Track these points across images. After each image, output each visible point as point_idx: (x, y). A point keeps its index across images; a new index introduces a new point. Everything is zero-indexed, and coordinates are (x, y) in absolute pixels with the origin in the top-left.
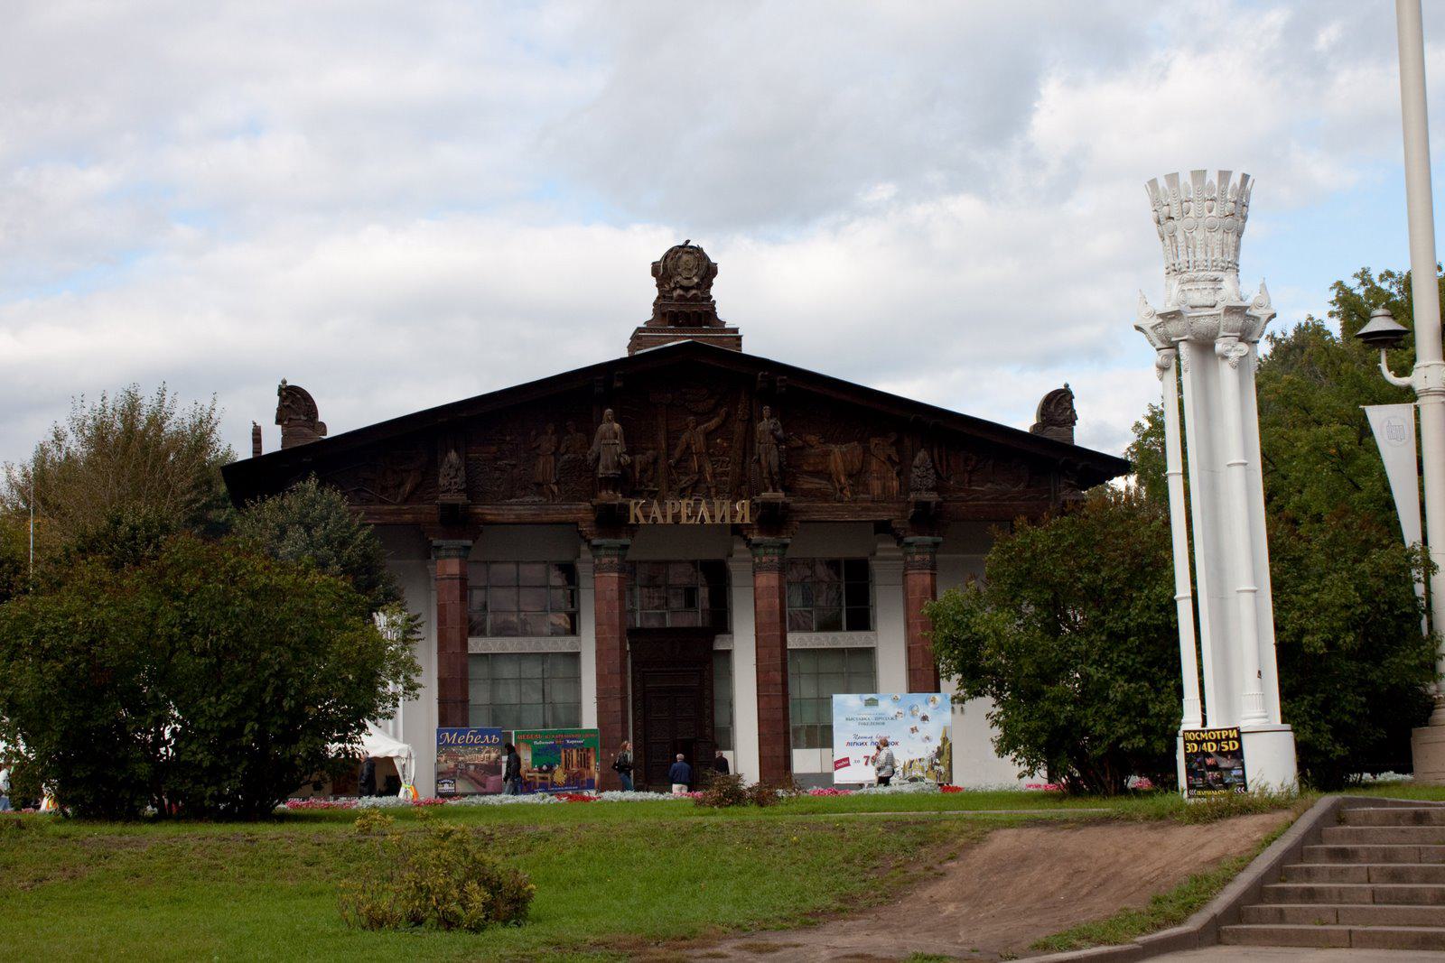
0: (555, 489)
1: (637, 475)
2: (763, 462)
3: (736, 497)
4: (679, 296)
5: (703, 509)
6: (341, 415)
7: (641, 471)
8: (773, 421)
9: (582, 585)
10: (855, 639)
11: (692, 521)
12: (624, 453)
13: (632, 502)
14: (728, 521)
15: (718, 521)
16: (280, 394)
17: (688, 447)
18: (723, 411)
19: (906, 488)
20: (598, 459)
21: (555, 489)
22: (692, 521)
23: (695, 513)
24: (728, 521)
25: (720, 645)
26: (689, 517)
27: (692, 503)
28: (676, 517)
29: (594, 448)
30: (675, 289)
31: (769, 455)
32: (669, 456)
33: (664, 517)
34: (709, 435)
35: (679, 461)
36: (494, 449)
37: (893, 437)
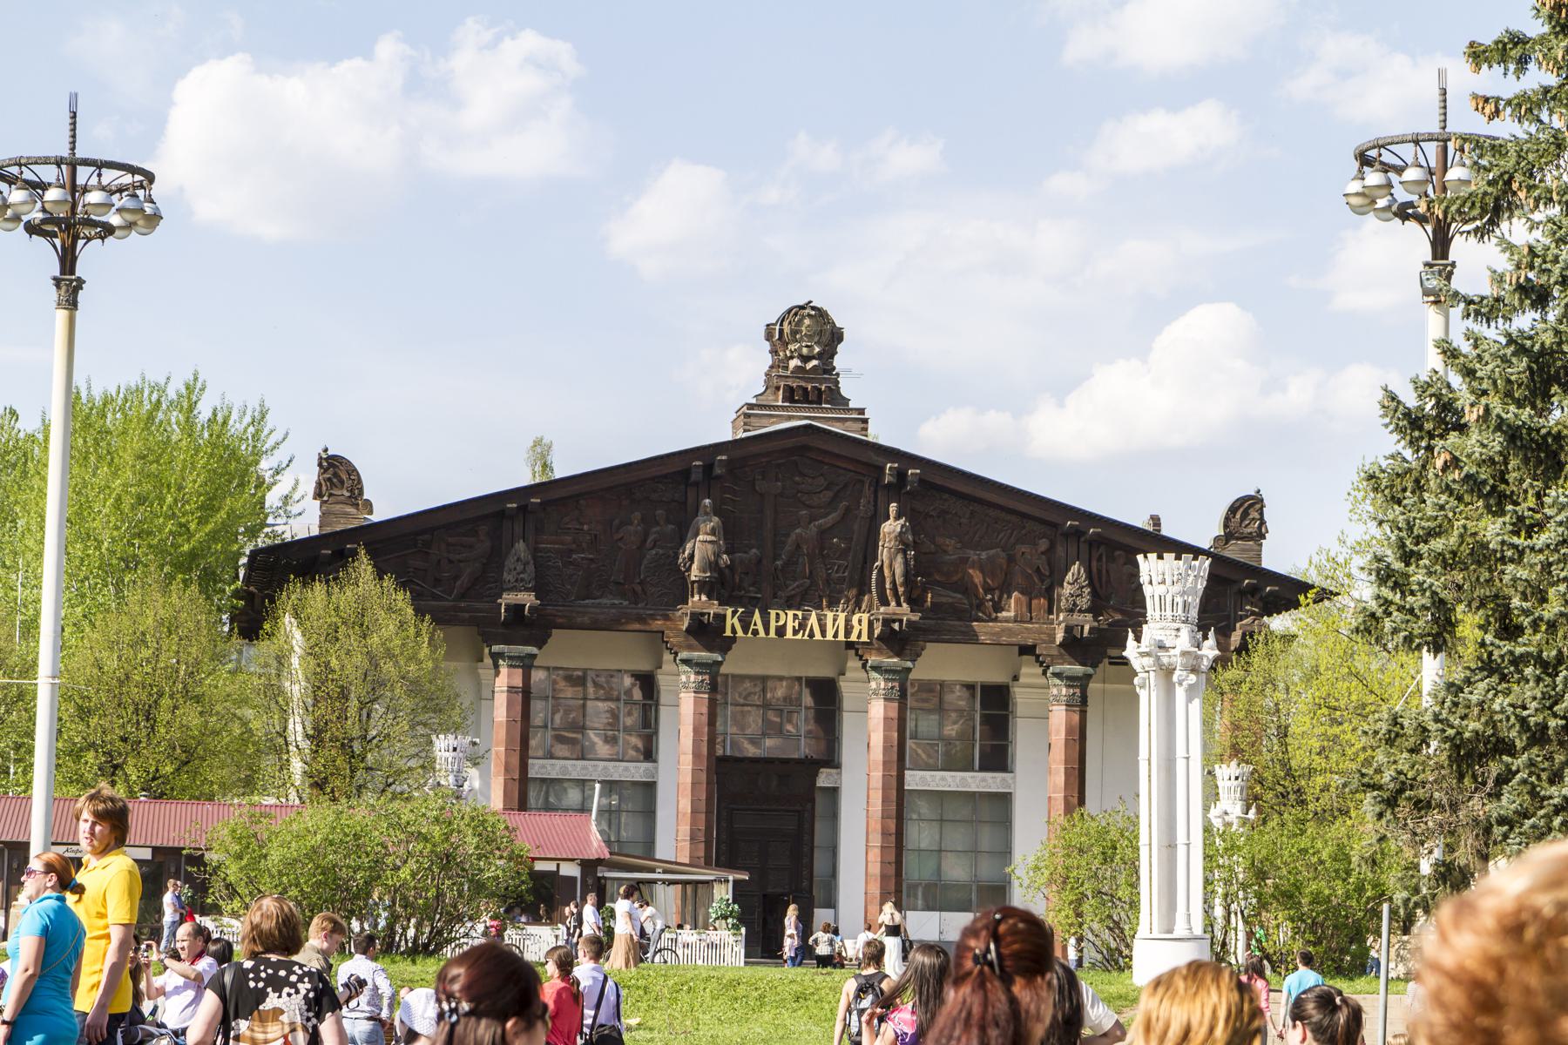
2: (886, 572)
4: (797, 367)
6: (391, 496)
8: (902, 521)
9: (663, 700)
10: (989, 782)
16: (320, 465)
22: (799, 636)
23: (802, 626)
24: (841, 637)
25: (824, 779)
26: (795, 632)
32: (776, 557)
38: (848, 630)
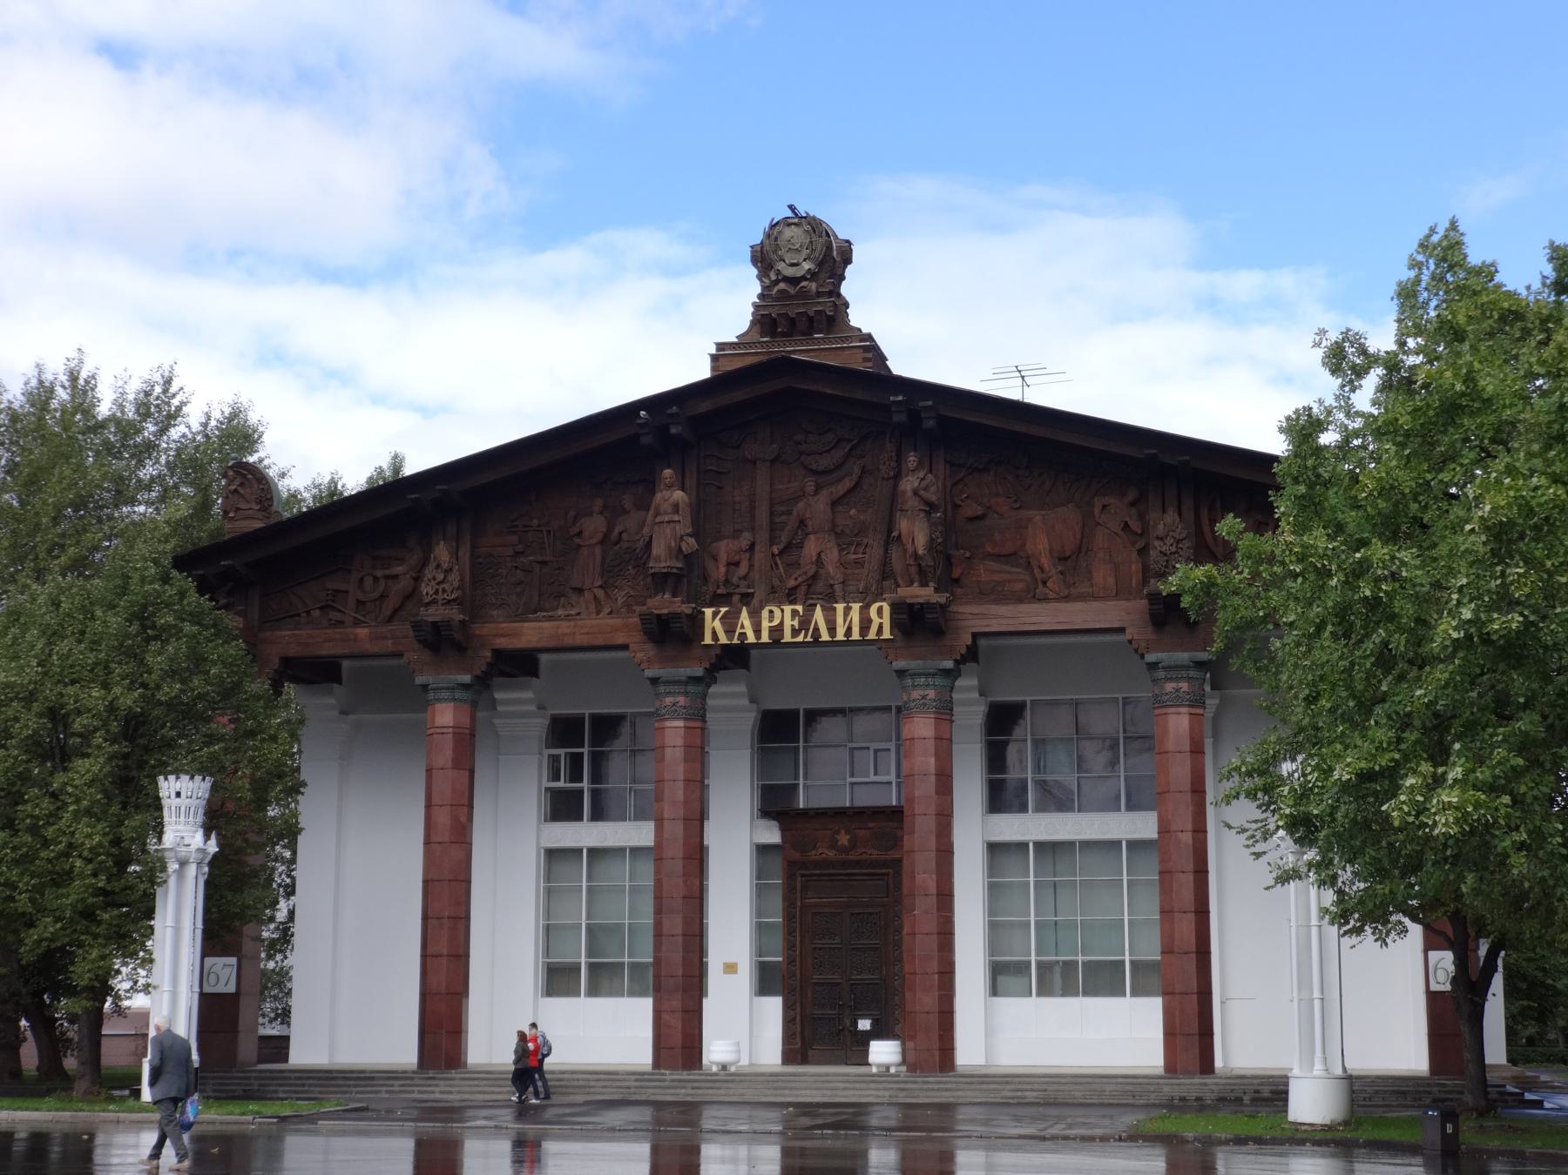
1: (723, 570)
5: (819, 615)
7: (729, 564)
11: (800, 639)
13: (708, 612)
14: (856, 636)
15: (840, 636)
19: (1147, 573)
20: (649, 545)
21: (600, 593)
23: (805, 623)
24: (856, 636)
26: (795, 632)
27: (800, 608)
28: (777, 631)
29: (646, 530)
30: (776, 282)
31: (917, 533)
33: (758, 632)
34: (834, 504)
35: (789, 546)
36: (514, 539)
37: (1132, 495)
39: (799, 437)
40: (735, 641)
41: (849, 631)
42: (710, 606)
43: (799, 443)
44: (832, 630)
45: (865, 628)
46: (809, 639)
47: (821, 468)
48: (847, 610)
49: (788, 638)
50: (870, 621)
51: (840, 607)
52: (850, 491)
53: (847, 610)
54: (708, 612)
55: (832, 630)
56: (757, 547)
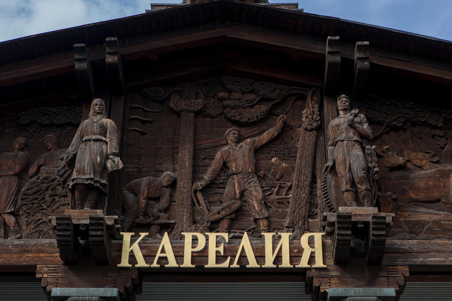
0: (11, 220)
1: (143, 202)
2: (340, 169)
3: (298, 227)
7: (149, 199)
11: (226, 264)
12: (114, 154)
13: (127, 236)
14: (286, 263)
15: (269, 263)
17: (225, 166)
18: (279, 123)
21: (11, 220)
26: (219, 258)
32: (195, 177)
33: (179, 257)
34: (258, 151)
38: (296, 254)
39: (221, 94)
40: (155, 264)
41: (278, 259)
42: (129, 231)
43: (221, 100)
44: (260, 257)
45: (296, 254)
46: (235, 265)
47: (245, 120)
48: (276, 240)
49: (212, 263)
50: (301, 250)
51: (268, 237)
52: (272, 142)
53: (276, 240)
54: (127, 236)
55: (260, 257)
56: (180, 184)
